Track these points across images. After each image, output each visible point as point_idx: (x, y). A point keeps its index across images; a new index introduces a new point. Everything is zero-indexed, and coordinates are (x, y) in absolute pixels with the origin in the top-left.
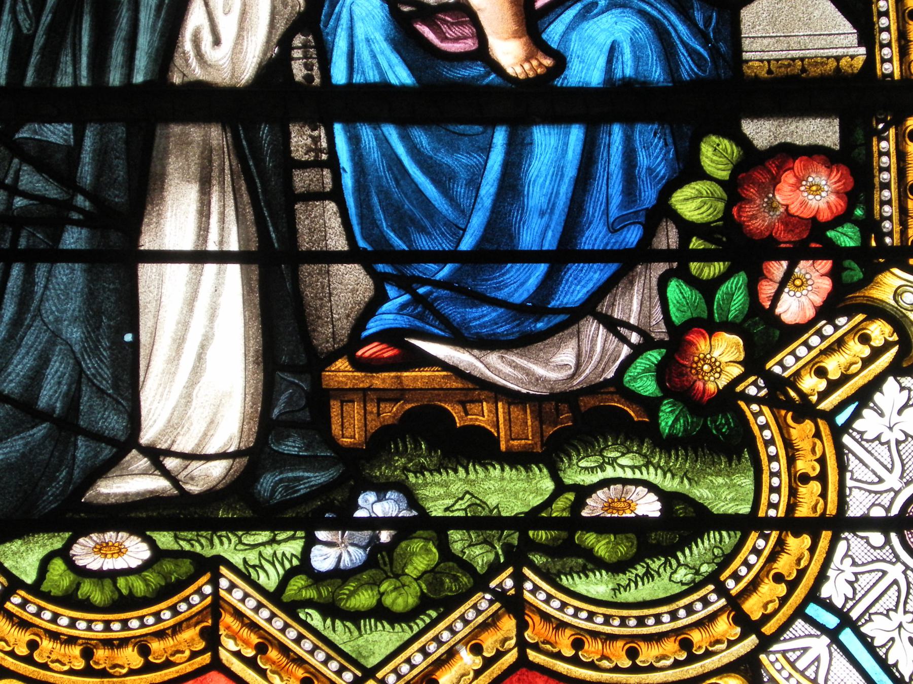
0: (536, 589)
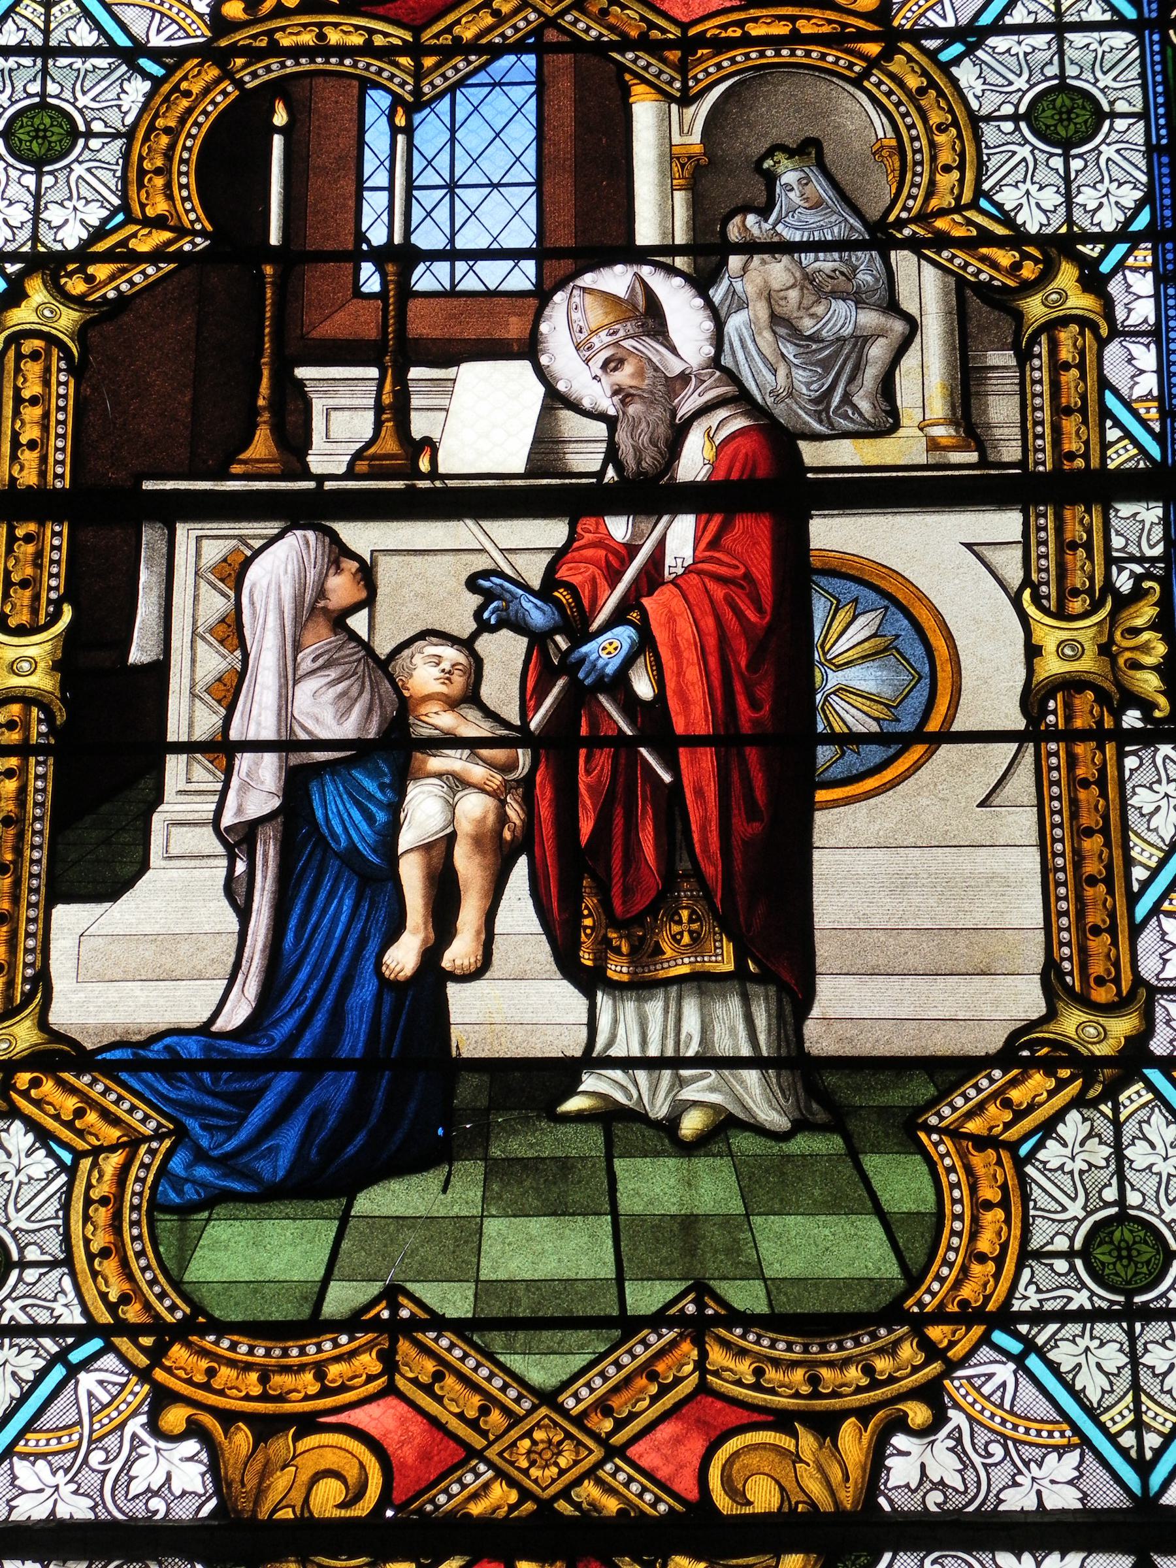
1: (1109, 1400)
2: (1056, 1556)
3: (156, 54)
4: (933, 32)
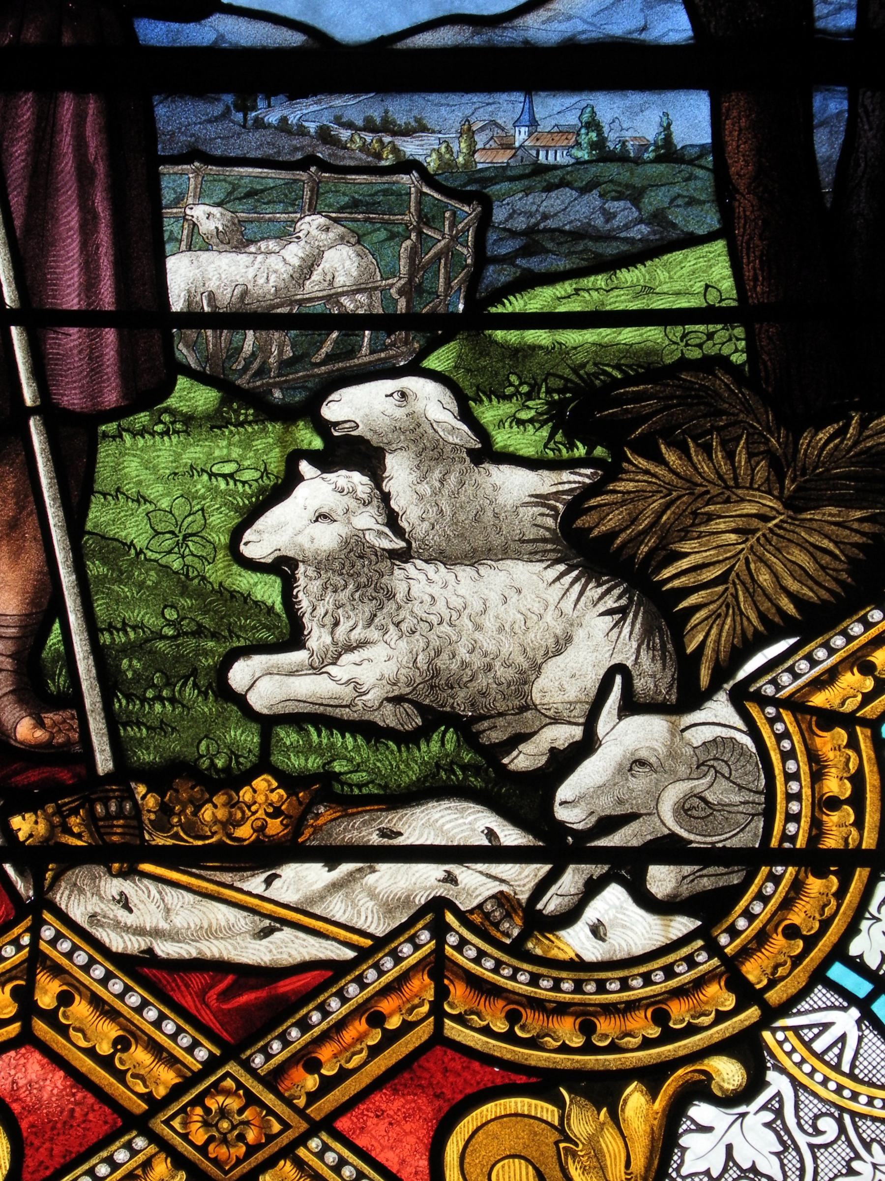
0: (463, 943)
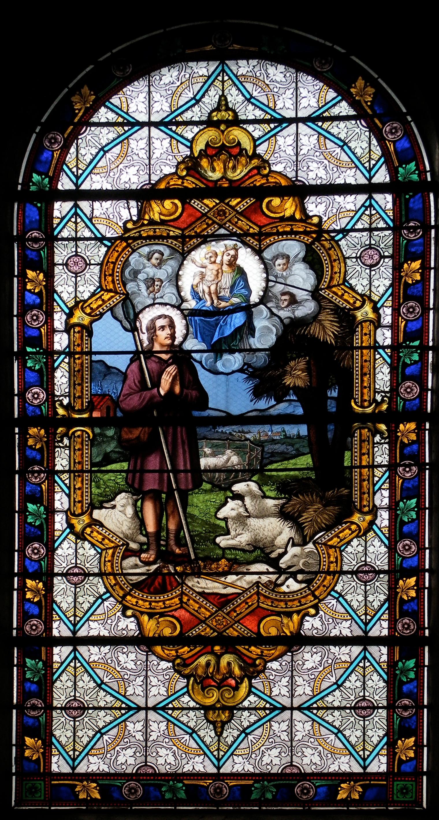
0: (262, 589)
1: (359, 608)
2: (344, 647)
3: (109, 239)
4: (334, 231)
